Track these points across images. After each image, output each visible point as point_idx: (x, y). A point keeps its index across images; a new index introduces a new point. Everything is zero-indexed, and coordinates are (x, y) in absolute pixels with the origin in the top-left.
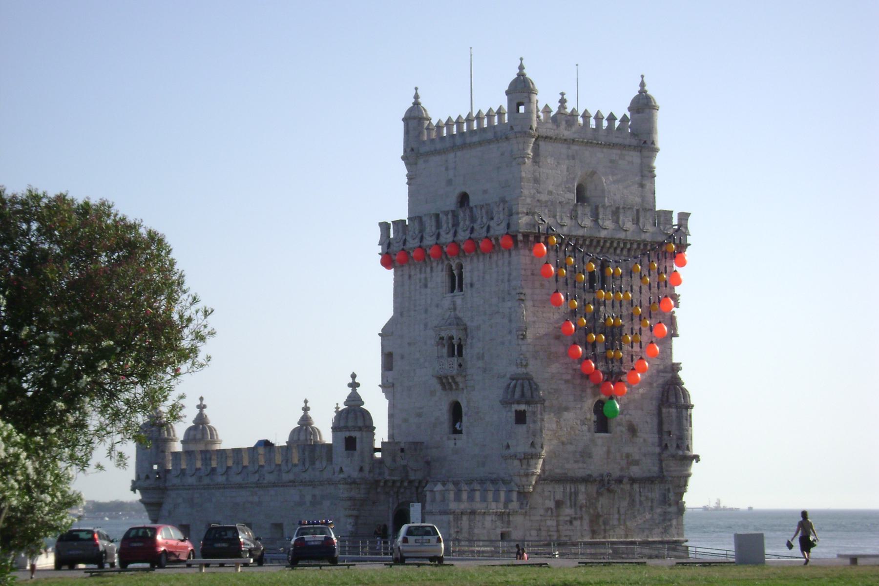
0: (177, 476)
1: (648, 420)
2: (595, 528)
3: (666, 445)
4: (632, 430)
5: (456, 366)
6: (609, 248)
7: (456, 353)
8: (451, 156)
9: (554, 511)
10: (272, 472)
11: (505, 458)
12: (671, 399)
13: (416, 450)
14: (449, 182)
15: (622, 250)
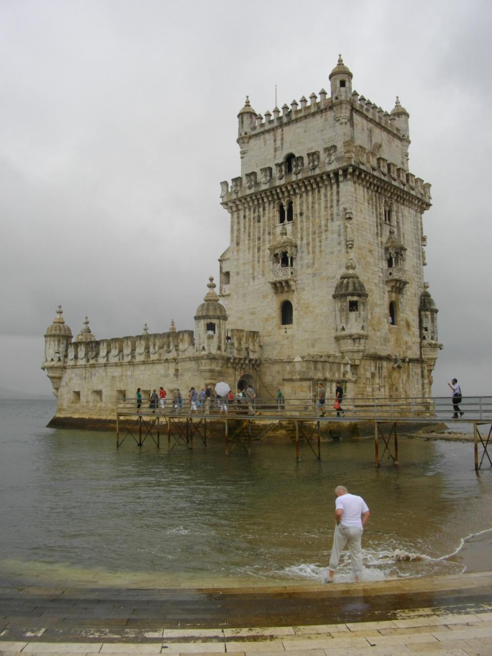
0: (72, 360)
1: (415, 319)
2: (392, 394)
3: (424, 338)
4: (408, 325)
5: (290, 274)
6: (395, 195)
7: (289, 263)
8: (279, 131)
9: (371, 379)
10: (142, 354)
11: (338, 339)
12: (426, 304)
13: (254, 336)
14: (276, 150)
15: (401, 198)
